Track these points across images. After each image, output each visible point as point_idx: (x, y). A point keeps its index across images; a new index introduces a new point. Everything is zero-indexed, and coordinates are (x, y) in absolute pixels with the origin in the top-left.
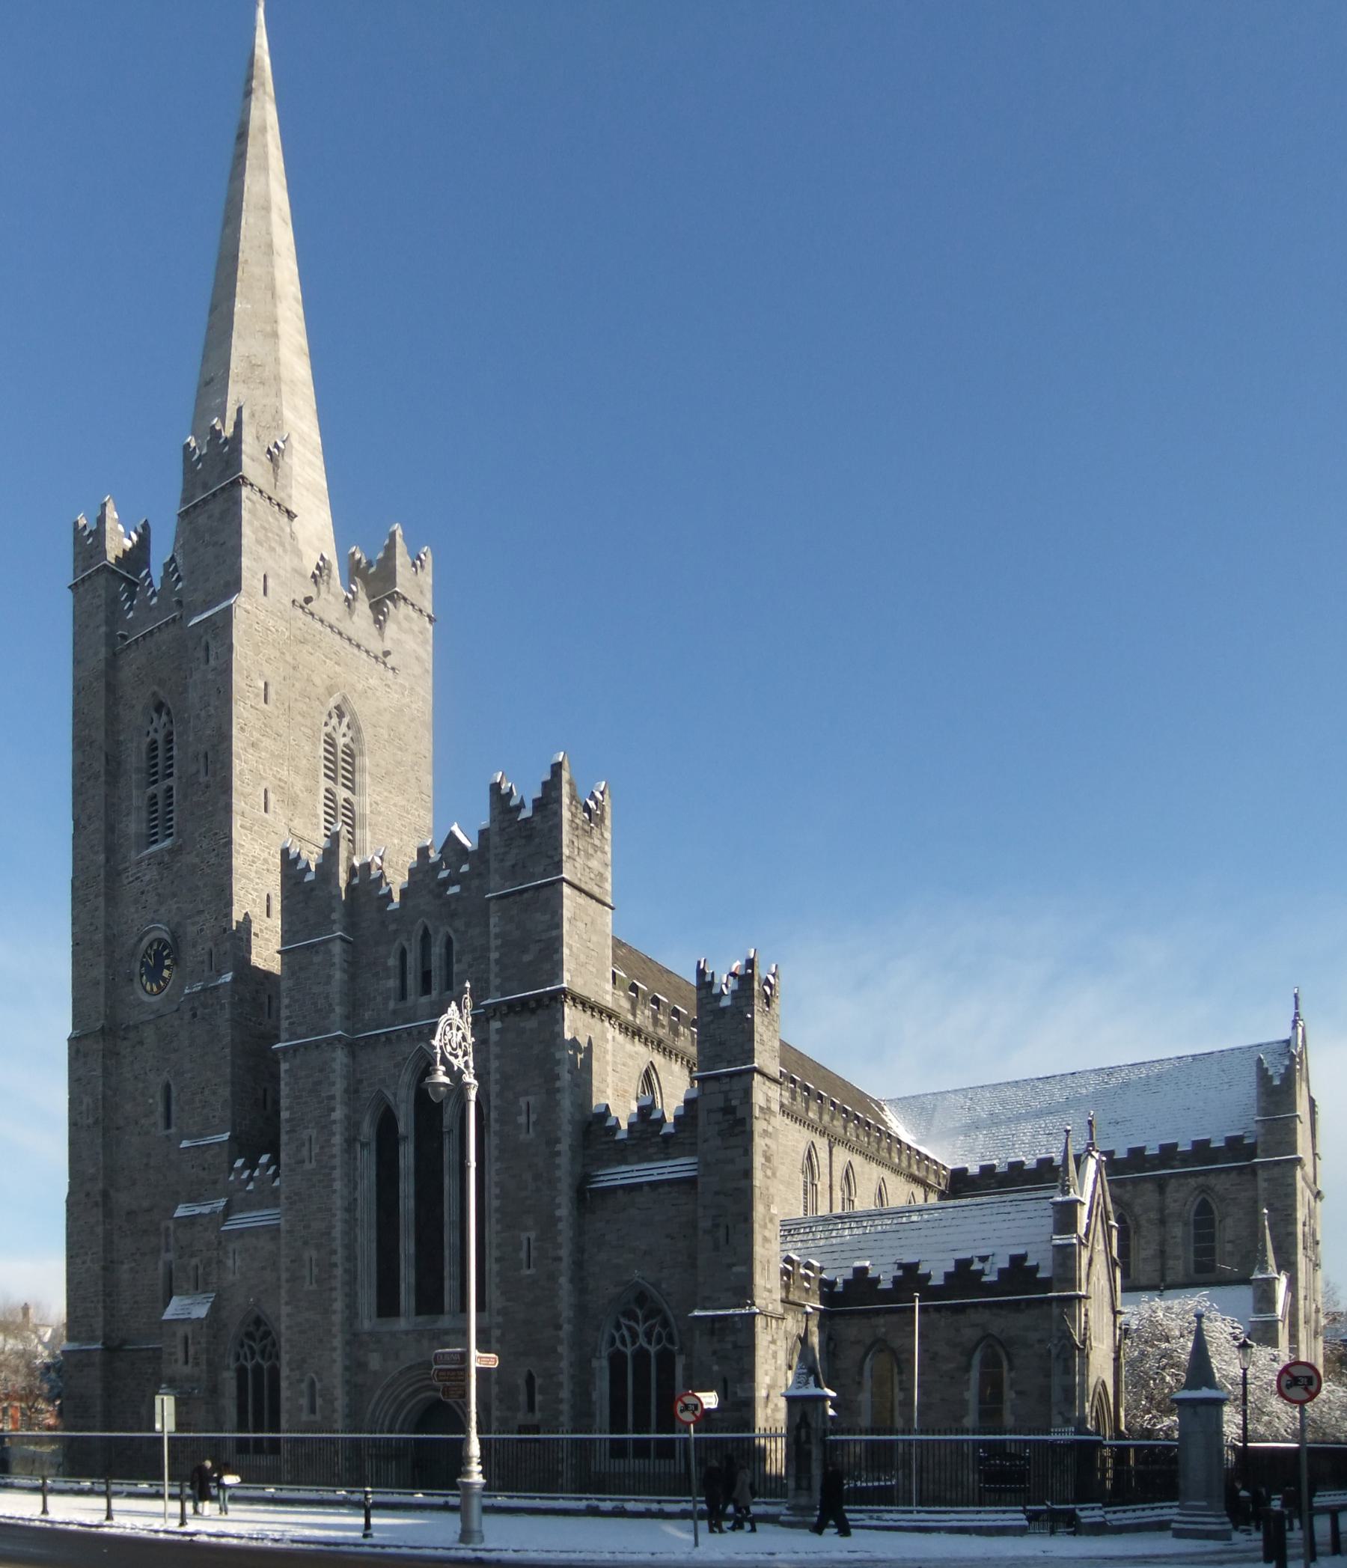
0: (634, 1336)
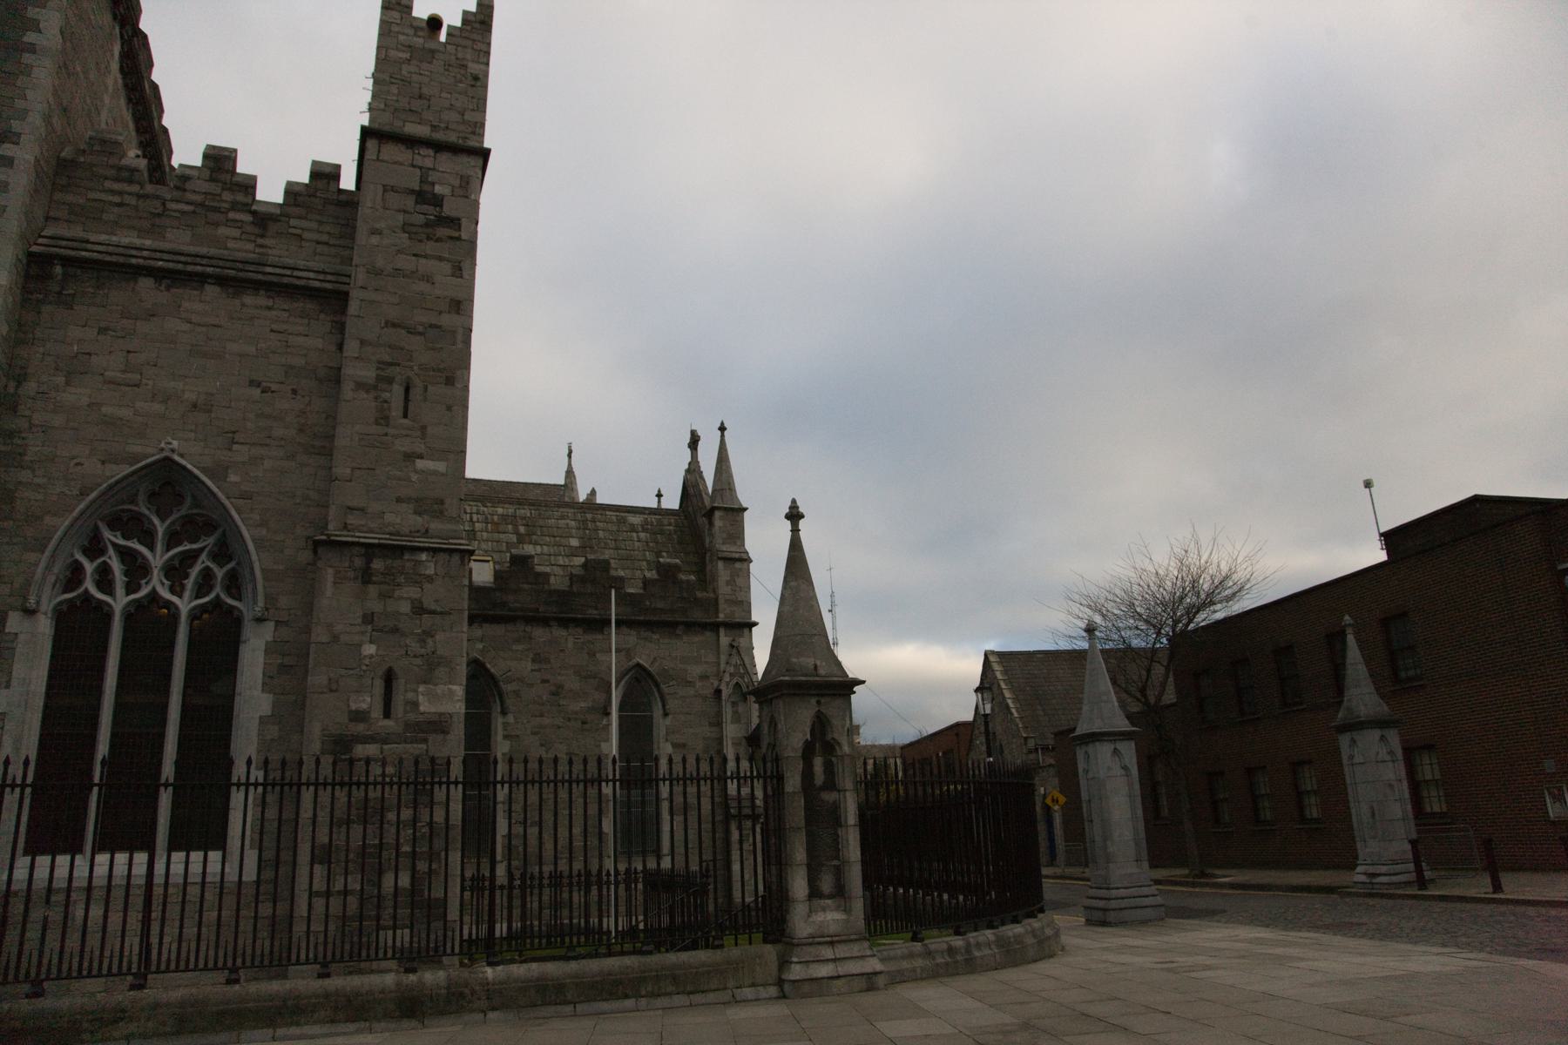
0: (137, 570)
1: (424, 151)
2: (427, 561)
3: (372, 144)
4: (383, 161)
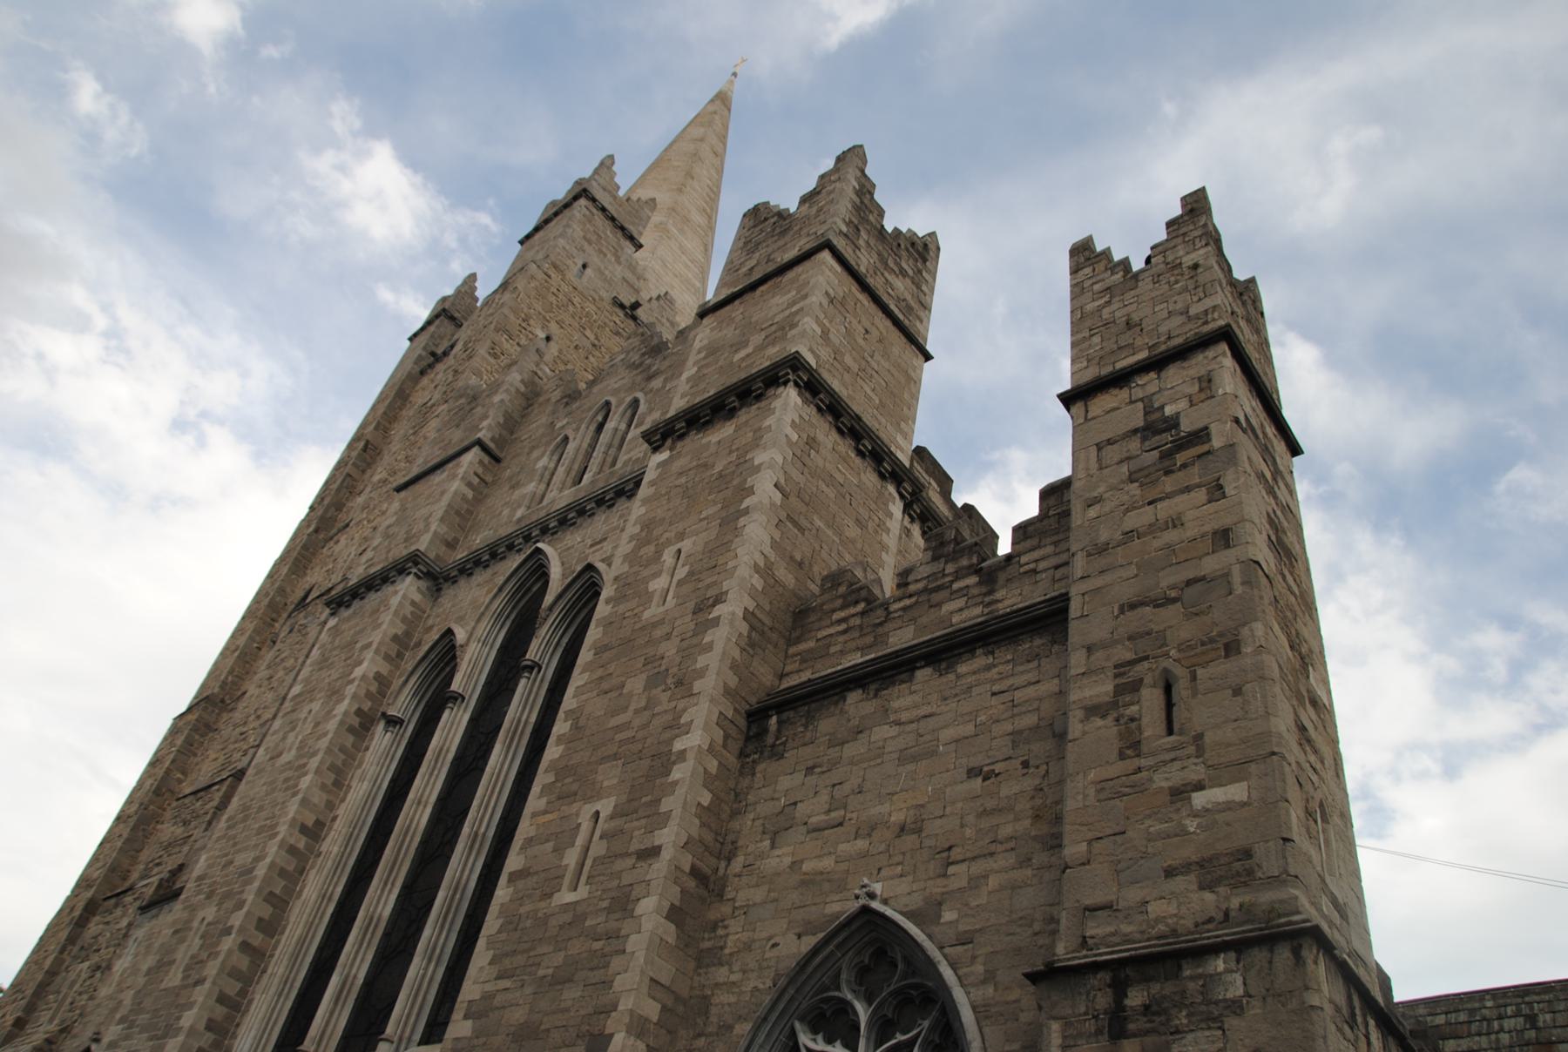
1: (1141, 380)
2: (1228, 971)
3: (1078, 407)
4: (1093, 418)
